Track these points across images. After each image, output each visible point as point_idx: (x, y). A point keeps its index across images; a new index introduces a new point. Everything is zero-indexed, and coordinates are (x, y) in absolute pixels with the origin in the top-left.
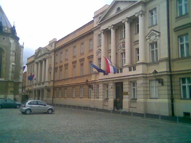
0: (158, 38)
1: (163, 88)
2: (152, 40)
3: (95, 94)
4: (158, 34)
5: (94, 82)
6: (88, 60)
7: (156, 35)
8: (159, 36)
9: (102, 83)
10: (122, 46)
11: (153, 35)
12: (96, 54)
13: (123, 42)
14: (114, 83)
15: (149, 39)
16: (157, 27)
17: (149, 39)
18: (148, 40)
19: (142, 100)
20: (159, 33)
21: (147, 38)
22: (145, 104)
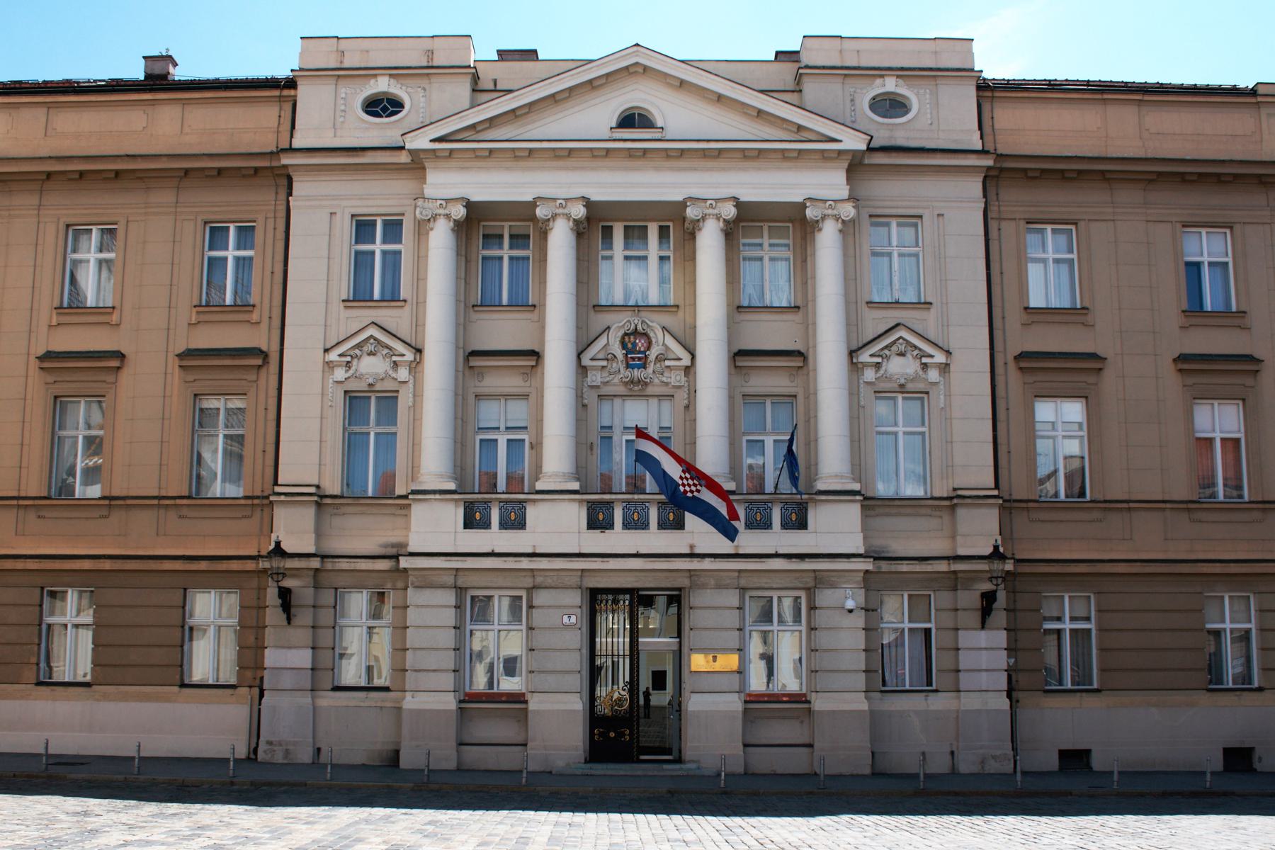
0: (933, 375)
1: (982, 638)
2: (902, 381)
3: (314, 659)
4: (940, 358)
5: (315, 563)
6: (176, 374)
7: (924, 360)
8: (944, 369)
10: (619, 353)
11: (902, 354)
13: (636, 333)
14: (587, 588)
15: (878, 366)
16: (933, 313)
17: (878, 366)
18: (869, 375)
19: (859, 703)
20: (948, 353)
21: (865, 357)
22: (875, 720)
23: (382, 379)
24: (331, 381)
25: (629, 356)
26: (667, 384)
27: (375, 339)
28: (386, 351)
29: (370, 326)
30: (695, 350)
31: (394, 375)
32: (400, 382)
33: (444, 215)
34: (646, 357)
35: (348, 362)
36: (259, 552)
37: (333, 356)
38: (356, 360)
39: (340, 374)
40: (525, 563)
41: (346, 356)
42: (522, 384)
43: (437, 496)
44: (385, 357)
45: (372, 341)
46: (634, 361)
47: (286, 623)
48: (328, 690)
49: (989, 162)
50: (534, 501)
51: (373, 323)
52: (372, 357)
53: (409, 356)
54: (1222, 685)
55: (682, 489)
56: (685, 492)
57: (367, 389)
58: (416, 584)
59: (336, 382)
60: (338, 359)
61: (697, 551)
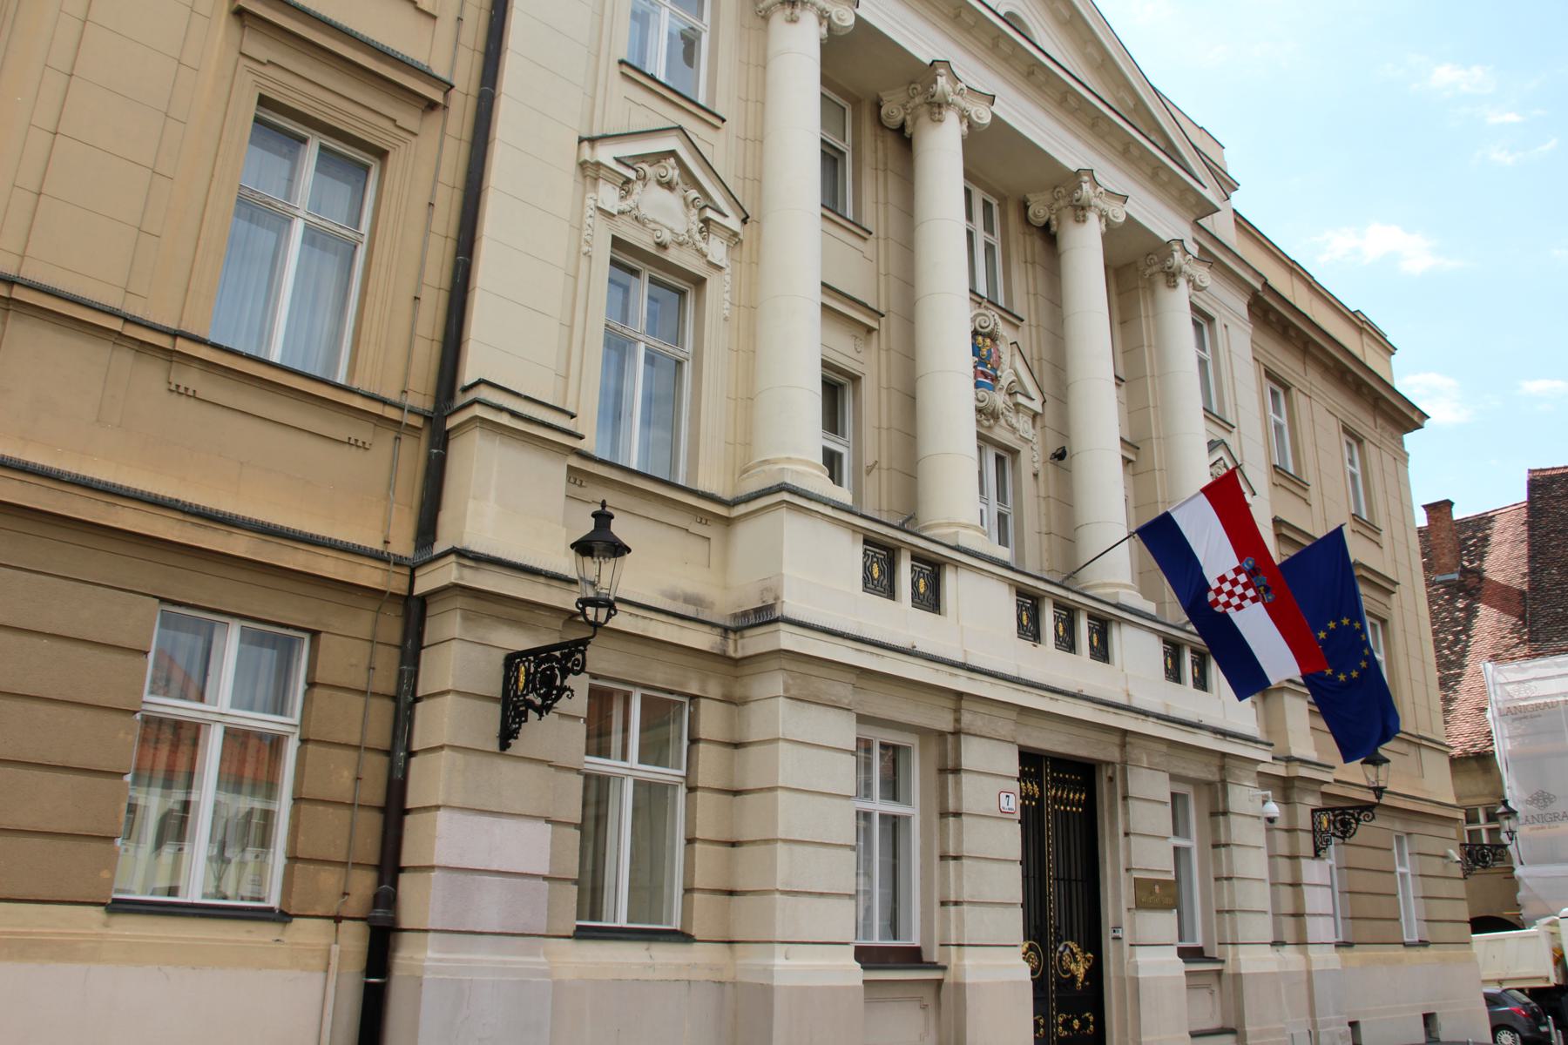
9: (842, 690)
12: (605, 154)
23: (680, 244)
24: (590, 203)
25: (979, 368)
26: (1014, 429)
27: (680, 163)
28: (693, 193)
29: (675, 133)
30: (1028, 393)
31: (702, 245)
32: (710, 264)
33: (818, 9)
34: (995, 379)
35: (628, 181)
36: (386, 542)
37: (605, 154)
38: (640, 183)
39: (608, 196)
40: (961, 683)
41: (629, 166)
42: (850, 351)
43: (829, 511)
44: (688, 204)
45: (672, 161)
46: (986, 378)
47: (494, 746)
48: (569, 937)
49: (1259, 286)
50: (957, 565)
51: (680, 128)
52: (665, 193)
53: (733, 222)
54: (601, 920)
55: (1211, 596)
56: (1216, 602)
57: (652, 250)
58: (793, 693)
59: (599, 209)
60: (614, 165)
61: (1136, 704)
